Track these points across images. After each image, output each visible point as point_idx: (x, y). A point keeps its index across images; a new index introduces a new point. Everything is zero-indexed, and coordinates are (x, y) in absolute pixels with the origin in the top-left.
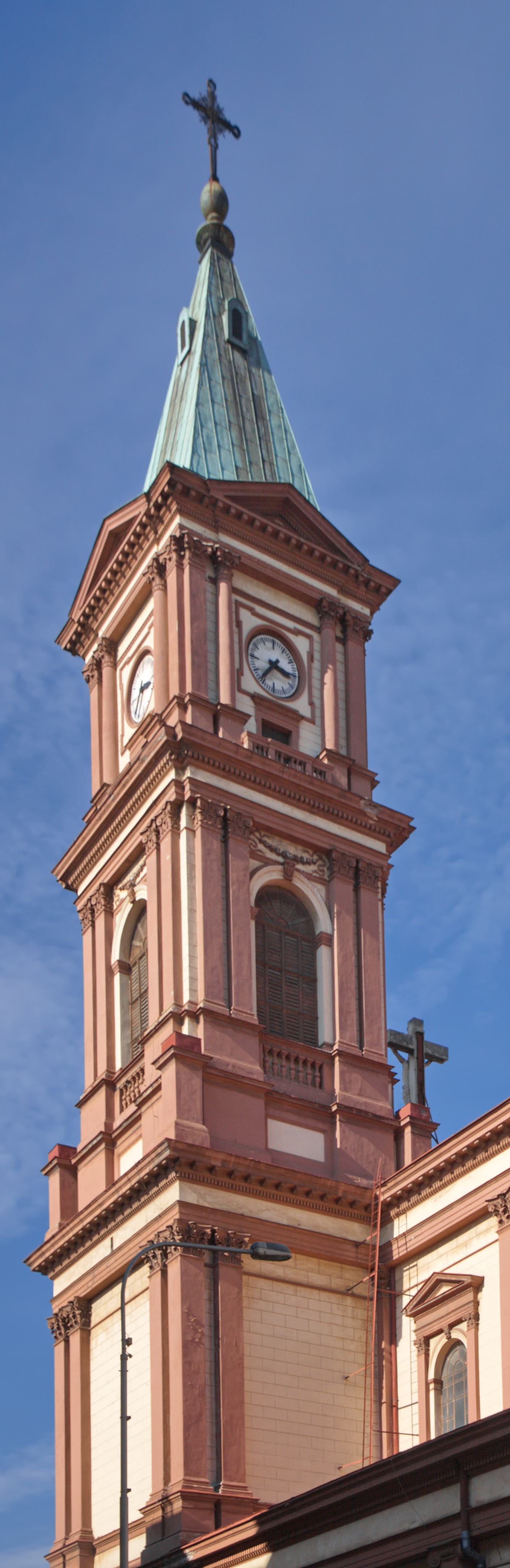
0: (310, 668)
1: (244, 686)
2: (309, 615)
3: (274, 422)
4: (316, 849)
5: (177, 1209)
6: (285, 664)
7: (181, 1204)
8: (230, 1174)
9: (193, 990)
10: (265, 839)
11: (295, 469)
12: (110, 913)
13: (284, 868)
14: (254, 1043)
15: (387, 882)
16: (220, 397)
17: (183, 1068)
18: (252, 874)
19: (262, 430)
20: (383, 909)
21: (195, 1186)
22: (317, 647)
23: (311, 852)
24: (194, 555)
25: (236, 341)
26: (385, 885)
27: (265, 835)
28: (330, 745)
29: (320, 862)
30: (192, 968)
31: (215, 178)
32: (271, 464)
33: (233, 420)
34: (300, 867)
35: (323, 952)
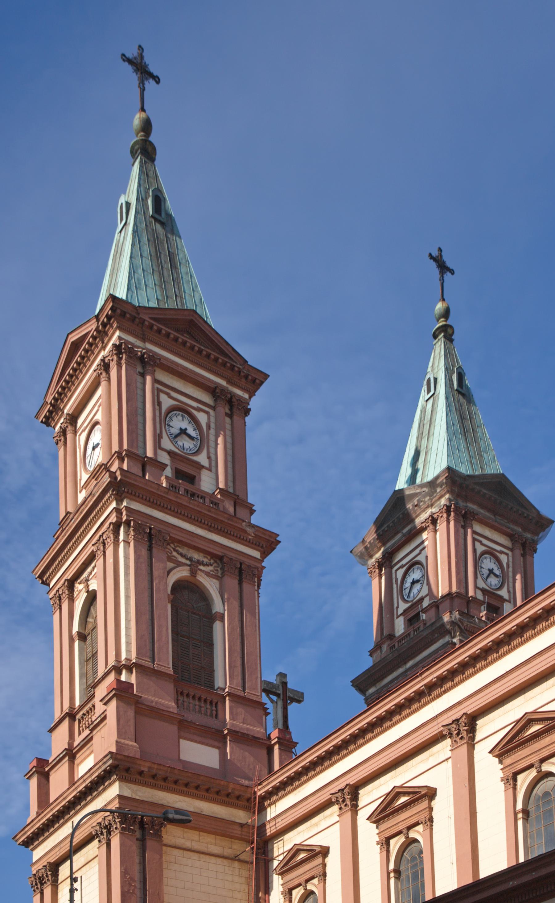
1: (163, 446)
2: (206, 398)
3: (183, 270)
4: (213, 556)
5: (117, 801)
6: (191, 431)
7: (120, 797)
8: (154, 777)
9: (128, 651)
10: (178, 548)
11: (197, 301)
12: (72, 599)
13: (191, 569)
14: (170, 687)
15: (261, 578)
16: (146, 253)
17: (121, 704)
18: (169, 572)
19: (175, 275)
20: (259, 597)
21: (129, 785)
22: (212, 419)
23: (209, 557)
24: (129, 357)
25: (157, 216)
26: (260, 580)
27: (178, 546)
28: (222, 485)
29: (215, 565)
30: (128, 635)
31: (143, 110)
32: (181, 298)
33: (155, 268)
34: (201, 567)
35: (217, 625)
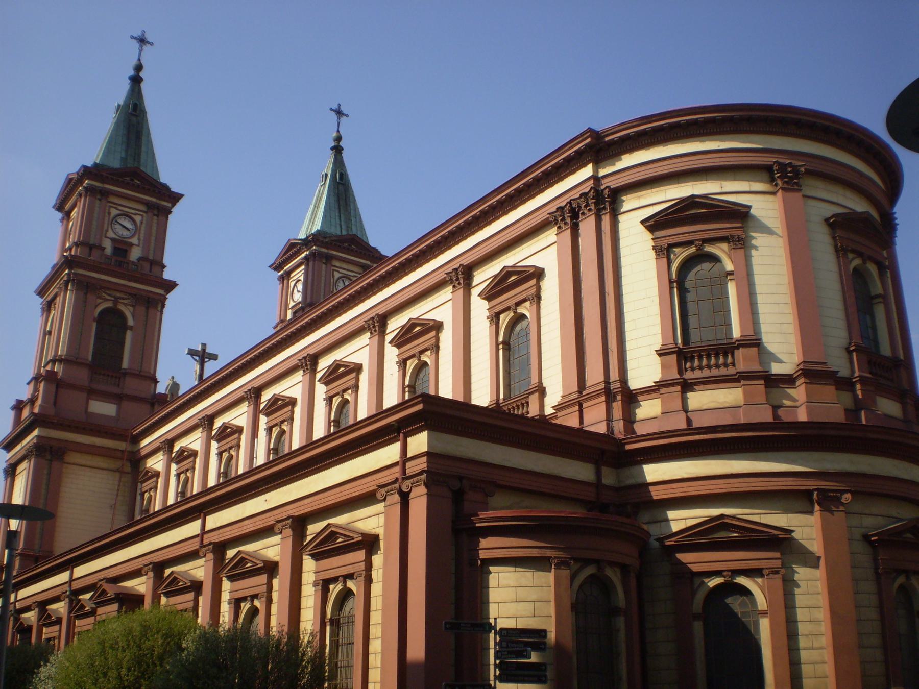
0: (140, 227)
4: (130, 294)
5: (35, 439)
7: (38, 437)
9: (62, 350)
29: (132, 299)
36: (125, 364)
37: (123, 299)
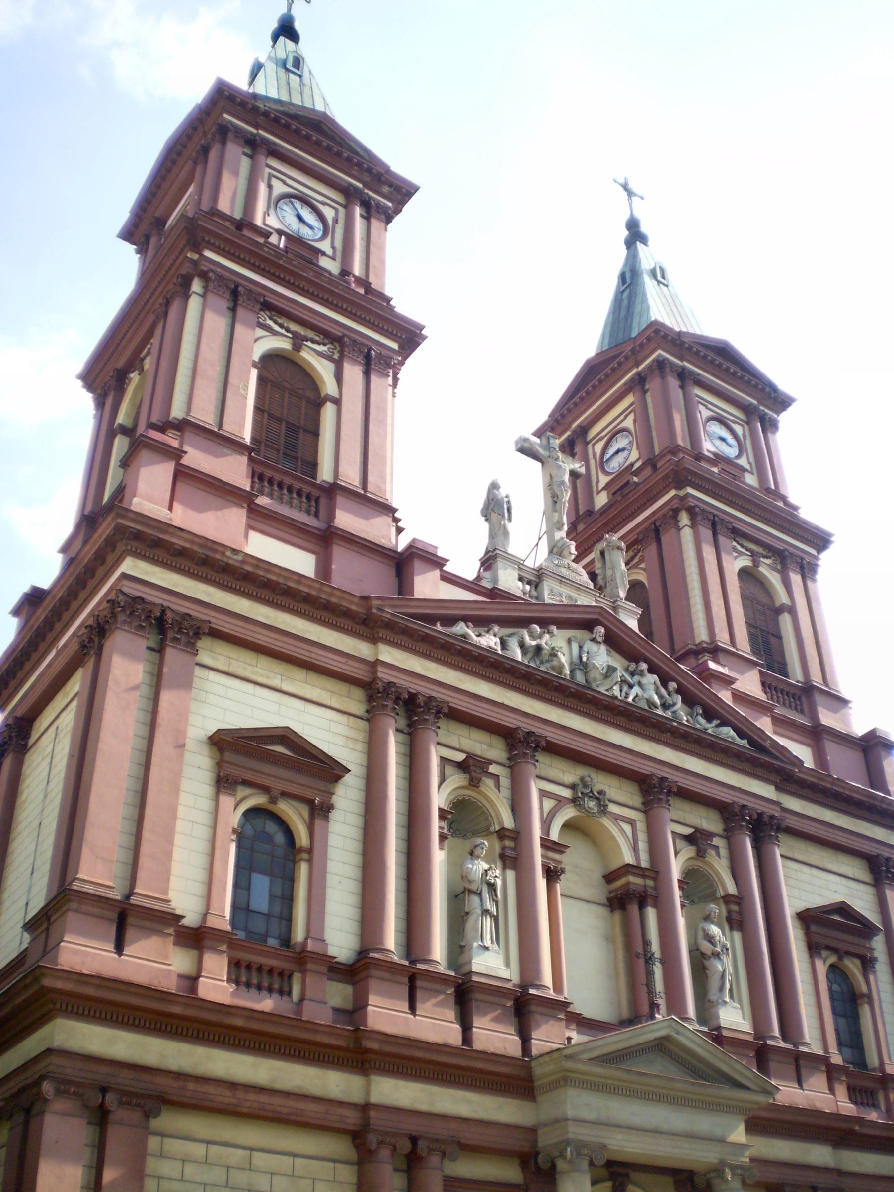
15: (398, 376)
27: (275, 315)
34: (309, 344)
36: (325, 474)
37: (313, 341)
